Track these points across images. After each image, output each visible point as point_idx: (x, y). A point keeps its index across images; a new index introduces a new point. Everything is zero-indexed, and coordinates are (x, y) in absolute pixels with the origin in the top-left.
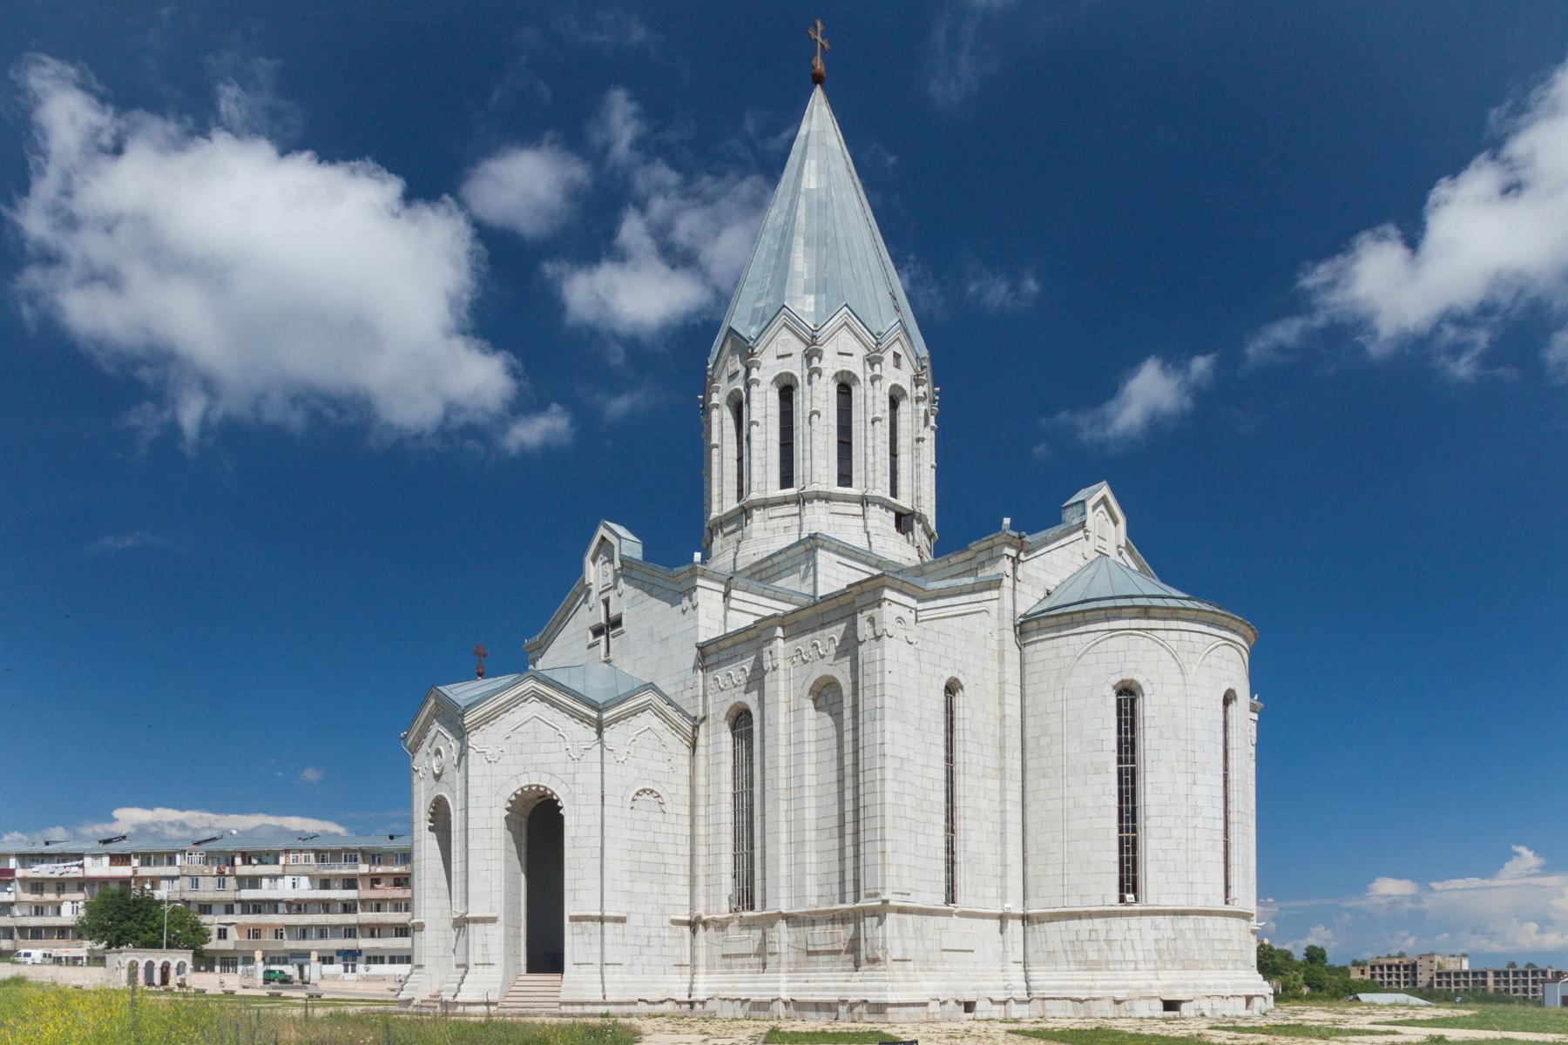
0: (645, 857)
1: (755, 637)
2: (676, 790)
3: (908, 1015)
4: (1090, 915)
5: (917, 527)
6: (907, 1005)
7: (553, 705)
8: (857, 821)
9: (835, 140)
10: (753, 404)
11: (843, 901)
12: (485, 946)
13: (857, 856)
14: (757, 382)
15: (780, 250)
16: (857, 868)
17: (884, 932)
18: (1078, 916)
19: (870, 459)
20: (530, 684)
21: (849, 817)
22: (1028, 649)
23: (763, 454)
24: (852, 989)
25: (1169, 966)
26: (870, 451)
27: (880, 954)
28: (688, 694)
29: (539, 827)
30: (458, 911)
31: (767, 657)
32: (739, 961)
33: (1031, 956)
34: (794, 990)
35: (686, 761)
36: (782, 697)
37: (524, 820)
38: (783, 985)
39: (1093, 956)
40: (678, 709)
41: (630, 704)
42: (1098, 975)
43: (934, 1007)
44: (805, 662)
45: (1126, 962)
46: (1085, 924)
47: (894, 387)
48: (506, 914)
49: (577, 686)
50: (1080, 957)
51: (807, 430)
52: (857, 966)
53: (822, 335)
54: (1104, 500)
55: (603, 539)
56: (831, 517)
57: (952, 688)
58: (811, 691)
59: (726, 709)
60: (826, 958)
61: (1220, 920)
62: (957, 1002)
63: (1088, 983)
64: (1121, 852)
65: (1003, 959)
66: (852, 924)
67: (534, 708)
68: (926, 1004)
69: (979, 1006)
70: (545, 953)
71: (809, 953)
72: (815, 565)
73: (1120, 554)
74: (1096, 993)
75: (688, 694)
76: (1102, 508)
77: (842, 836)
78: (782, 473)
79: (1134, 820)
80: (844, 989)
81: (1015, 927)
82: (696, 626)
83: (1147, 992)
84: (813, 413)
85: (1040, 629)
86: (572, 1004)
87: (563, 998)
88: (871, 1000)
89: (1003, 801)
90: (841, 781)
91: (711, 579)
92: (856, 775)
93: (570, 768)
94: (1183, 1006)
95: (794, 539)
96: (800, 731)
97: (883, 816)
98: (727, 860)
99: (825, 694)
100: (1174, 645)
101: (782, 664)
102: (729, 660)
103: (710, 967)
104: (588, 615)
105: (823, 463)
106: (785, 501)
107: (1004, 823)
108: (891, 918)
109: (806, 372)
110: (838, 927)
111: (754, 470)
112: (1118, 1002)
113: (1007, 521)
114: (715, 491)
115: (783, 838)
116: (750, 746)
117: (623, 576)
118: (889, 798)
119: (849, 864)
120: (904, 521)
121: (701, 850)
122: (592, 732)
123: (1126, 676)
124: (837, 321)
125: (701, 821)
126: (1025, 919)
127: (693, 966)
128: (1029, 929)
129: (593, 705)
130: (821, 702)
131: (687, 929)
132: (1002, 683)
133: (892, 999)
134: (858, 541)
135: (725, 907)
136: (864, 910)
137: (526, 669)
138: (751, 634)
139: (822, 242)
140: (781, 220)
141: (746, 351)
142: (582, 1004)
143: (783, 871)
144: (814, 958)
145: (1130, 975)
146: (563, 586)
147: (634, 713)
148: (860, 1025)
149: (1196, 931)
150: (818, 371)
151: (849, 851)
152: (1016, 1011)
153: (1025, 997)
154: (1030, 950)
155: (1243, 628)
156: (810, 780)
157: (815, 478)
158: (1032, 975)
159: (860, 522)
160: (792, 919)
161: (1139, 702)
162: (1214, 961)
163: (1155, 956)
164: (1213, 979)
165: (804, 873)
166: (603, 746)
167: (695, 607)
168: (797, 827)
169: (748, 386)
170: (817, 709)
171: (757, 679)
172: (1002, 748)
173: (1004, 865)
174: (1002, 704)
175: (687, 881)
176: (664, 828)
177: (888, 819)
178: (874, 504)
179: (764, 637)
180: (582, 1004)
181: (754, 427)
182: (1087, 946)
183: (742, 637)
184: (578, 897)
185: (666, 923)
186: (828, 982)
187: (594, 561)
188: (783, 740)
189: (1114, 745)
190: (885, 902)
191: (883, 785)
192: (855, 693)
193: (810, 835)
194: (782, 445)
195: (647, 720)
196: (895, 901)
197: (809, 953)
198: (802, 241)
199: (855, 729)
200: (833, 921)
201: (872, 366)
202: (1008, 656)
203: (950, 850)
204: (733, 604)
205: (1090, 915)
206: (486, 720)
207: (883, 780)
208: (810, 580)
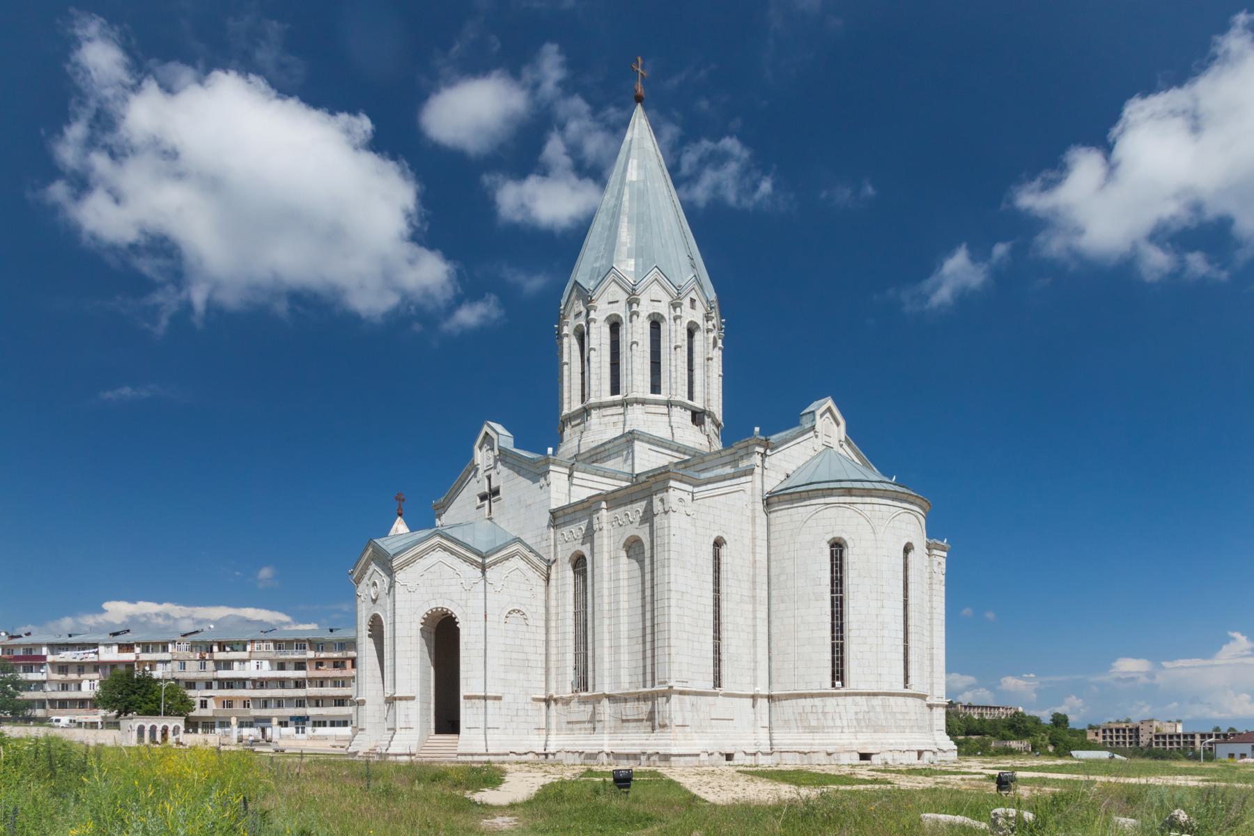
0: (514, 655)
1: (587, 508)
4: (812, 696)
5: (708, 420)
7: (452, 553)
12: (407, 716)
13: (653, 657)
16: (653, 664)
18: (804, 696)
19: (673, 375)
20: (437, 539)
21: (648, 630)
22: (772, 515)
26: (673, 369)
27: (667, 722)
28: (544, 544)
29: (443, 635)
30: (389, 692)
31: (595, 521)
32: (578, 726)
33: (774, 724)
35: (542, 590)
36: (605, 548)
37: (433, 631)
39: (814, 723)
40: (537, 555)
41: (504, 552)
42: (817, 736)
43: (704, 757)
46: (809, 701)
47: (691, 323)
49: (468, 540)
50: (806, 724)
52: (653, 729)
53: (639, 289)
54: (829, 410)
55: (487, 433)
57: (718, 543)
58: (625, 545)
60: (634, 724)
61: (901, 699)
65: (754, 725)
66: (650, 701)
68: (698, 755)
69: (736, 757)
70: (447, 721)
71: (623, 721)
72: (633, 452)
74: (815, 748)
75: (544, 544)
76: (828, 415)
77: (644, 643)
78: (612, 384)
81: (763, 703)
84: (633, 343)
88: (661, 752)
89: (755, 618)
90: (643, 606)
91: (560, 465)
92: (653, 603)
93: (464, 596)
94: (873, 757)
95: (619, 433)
96: (617, 572)
98: (570, 657)
99: (633, 547)
100: (868, 513)
101: (605, 526)
102: (571, 522)
103: (559, 730)
104: (477, 486)
105: (641, 377)
106: (614, 404)
107: (755, 633)
108: (674, 698)
111: (592, 382)
112: (829, 754)
114: (566, 395)
115: (607, 643)
118: (673, 619)
119: (649, 662)
120: (698, 417)
121: (553, 651)
123: (836, 535)
124: (650, 278)
125: (553, 631)
127: (548, 729)
129: (479, 554)
130: (631, 553)
131: (543, 705)
132: (754, 539)
133: (674, 751)
134: (664, 433)
135: (569, 689)
137: (433, 525)
138: (586, 505)
139: (642, 222)
140: (612, 202)
141: (587, 298)
142: (472, 755)
143: (606, 666)
145: (838, 736)
147: (507, 558)
149: (883, 706)
151: (649, 653)
154: (773, 719)
155: (918, 501)
156: (624, 605)
157: (635, 389)
159: (666, 418)
160: (612, 698)
162: (896, 727)
163: (855, 723)
164: (895, 739)
168: (616, 636)
169: (588, 323)
171: (589, 536)
172: (754, 582)
173: (755, 662)
174: (754, 553)
175: (543, 671)
176: (527, 636)
180: (472, 755)
183: (580, 507)
184: (469, 683)
185: (529, 700)
188: (606, 577)
190: (671, 687)
192: (652, 548)
193: (624, 642)
195: (516, 562)
197: (623, 721)
199: (652, 572)
200: (638, 700)
201: (675, 309)
202: (758, 521)
203: (717, 651)
204: (575, 481)
205: (812, 696)
206: (407, 563)
208: (630, 462)
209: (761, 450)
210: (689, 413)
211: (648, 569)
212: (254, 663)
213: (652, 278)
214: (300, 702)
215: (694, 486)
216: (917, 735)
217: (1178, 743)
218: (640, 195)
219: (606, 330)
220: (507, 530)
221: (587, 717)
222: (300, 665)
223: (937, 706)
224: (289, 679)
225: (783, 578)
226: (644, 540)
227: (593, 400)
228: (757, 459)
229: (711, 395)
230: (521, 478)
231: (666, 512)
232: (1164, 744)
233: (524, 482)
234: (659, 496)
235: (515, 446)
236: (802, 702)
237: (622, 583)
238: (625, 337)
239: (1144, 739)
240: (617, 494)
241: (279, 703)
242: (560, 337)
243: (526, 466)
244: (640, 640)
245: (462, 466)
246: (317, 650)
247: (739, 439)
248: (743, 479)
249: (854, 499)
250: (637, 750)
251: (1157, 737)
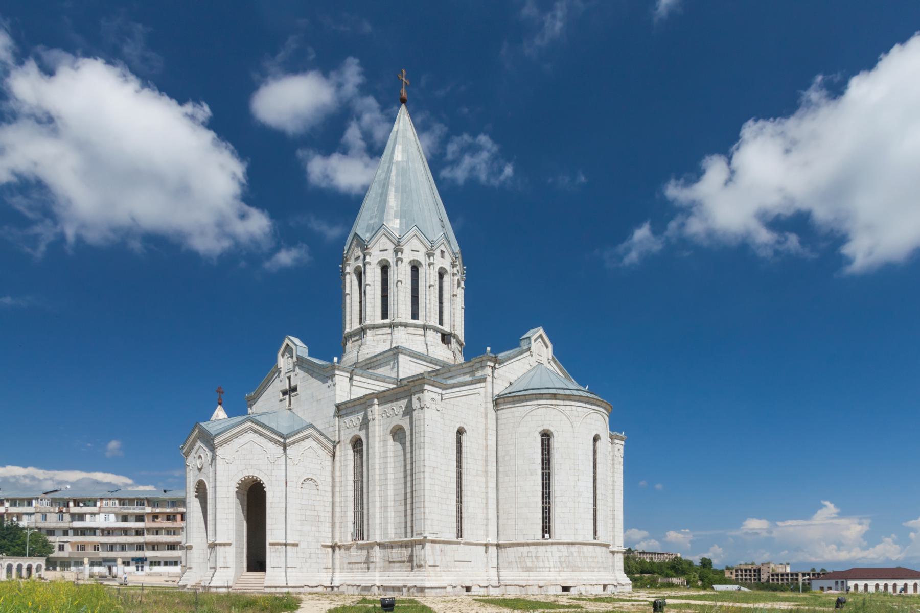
0: (308, 513)
1: (364, 403)
3: (436, 593)
4: (528, 544)
5: (453, 341)
7: (261, 435)
9: (412, 134)
10: (367, 274)
12: (225, 558)
13: (412, 515)
14: (369, 263)
15: (382, 193)
16: (412, 520)
18: (522, 545)
19: (428, 306)
21: (409, 495)
22: (500, 412)
27: (423, 563)
28: (331, 429)
29: (253, 497)
30: (211, 540)
31: (369, 413)
32: (356, 566)
35: (330, 464)
36: (377, 434)
37: (246, 493)
39: (529, 564)
40: (326, 437)
42: (531, 574)
43: (449, 589)
46: (526, 549)
47: (441, 268)
48: (236, 541)
49: (273, 425)
50: (524, 565)
52: (412, 568)
57: (460, 432)
58: (391, 432)
66: (409, 548)
67: (251, 436)
69: (473, 589)
70: (257, 563)
72: (398, 362)
74: (530, 583)
75: (331, 429)
77: (406, 504)
78: (383, 311)
81: (493, 549)
83: (554, 582)
84: (398, 281)
85: (505, 403)
86: (270, 587)
87: (266, 585)
88: (418, 585)
89: (487, 487)
90: (405, 477)
91: (343, 371)
92: (412, 475)
95: (388, 348)
96: (386, 451)
98: (350, 514)
99: (398, 433)
101: (377, 417)
103: (342, 569)
104: (278, 385)
105: (404, 307)
106: (384, 326)
107: (487, 498)
108: (428, 545)
109: (395, 260)
111: (368, 309)
112: (540, 587)
113: (489, 349)
115: (378, 504)
118: (427, 487)
120: (446, 338)
121: (337, 509)
122: (281, 449)
124: (411, 234)
125: (337, 494)
126: (498, 546)
129: (281, 436)
130: (396, 437)
131: (330, 550)
132: (486, 429)
133: (428, 584)
134: (421, 349)
135: (349, 538)
137: (246, 413)
138: (362, 401)
139: (405, 191)
140: (383, 176)
142: (275, 587)
143: (378, 521)
147: (303, 439)
151: (409, 512)
154: (500, 561)
156: (391, 476)
157: (399, 315)
159: (423, 338)
160: (381, 545)
161: (552, 440)
165: (387, 522)
168: (384, 499)
169: (365, 265)
171: (365, 424)
172: (486, 461)
173: (487, 519)
174: (486, 440)
175: (330, 525)
180: (275, 587)
181: (368, 287)
182: (527, 560)
184: (274, 532)
185: (319, 546)
188: (377, 455)
190: (425, 538)
192: (412, 434)
193: (391, 503)
195: (310, 443)
196: (430, 537)
199: (412, 452)
200: (401, 546)
201: (429, 257)
202: (489, 416)
203: (459, 511)
204: (354, 383)
205: (528, 544)
208: (395, 369)
209: (492, 364)
210: (440, 335)
211: (408, 449)
212: (102, 516)
213: (413, 234)
214: (140, 547)
215: (443, 389)
217: (787, 580)
218: (404, 172)
219: (378, 271)
220: (303, 418)
221: (363, 559)
222: (140, 518)
223: (618, 552)
224: (130, 529)
225: (507, 458)
227: (368, 322)
228: (488, 371)
229: (456, 322)
230: (314, 380)
231: (422, 408)
232: (778, 580)
233: (316, 383)
234: (417, 396)
235: (309, 355)
236: (521, 549)
237: (389, 460)
238: (392, 277)
239: (764, 577)
240: (386, 394)
241: (123, 547)
242: (344, 274)
243: (317, 371)
244: (403, 502)
245: (269, 369)
248: (478, 385)
250: (400, 584)
251: (773, 575)
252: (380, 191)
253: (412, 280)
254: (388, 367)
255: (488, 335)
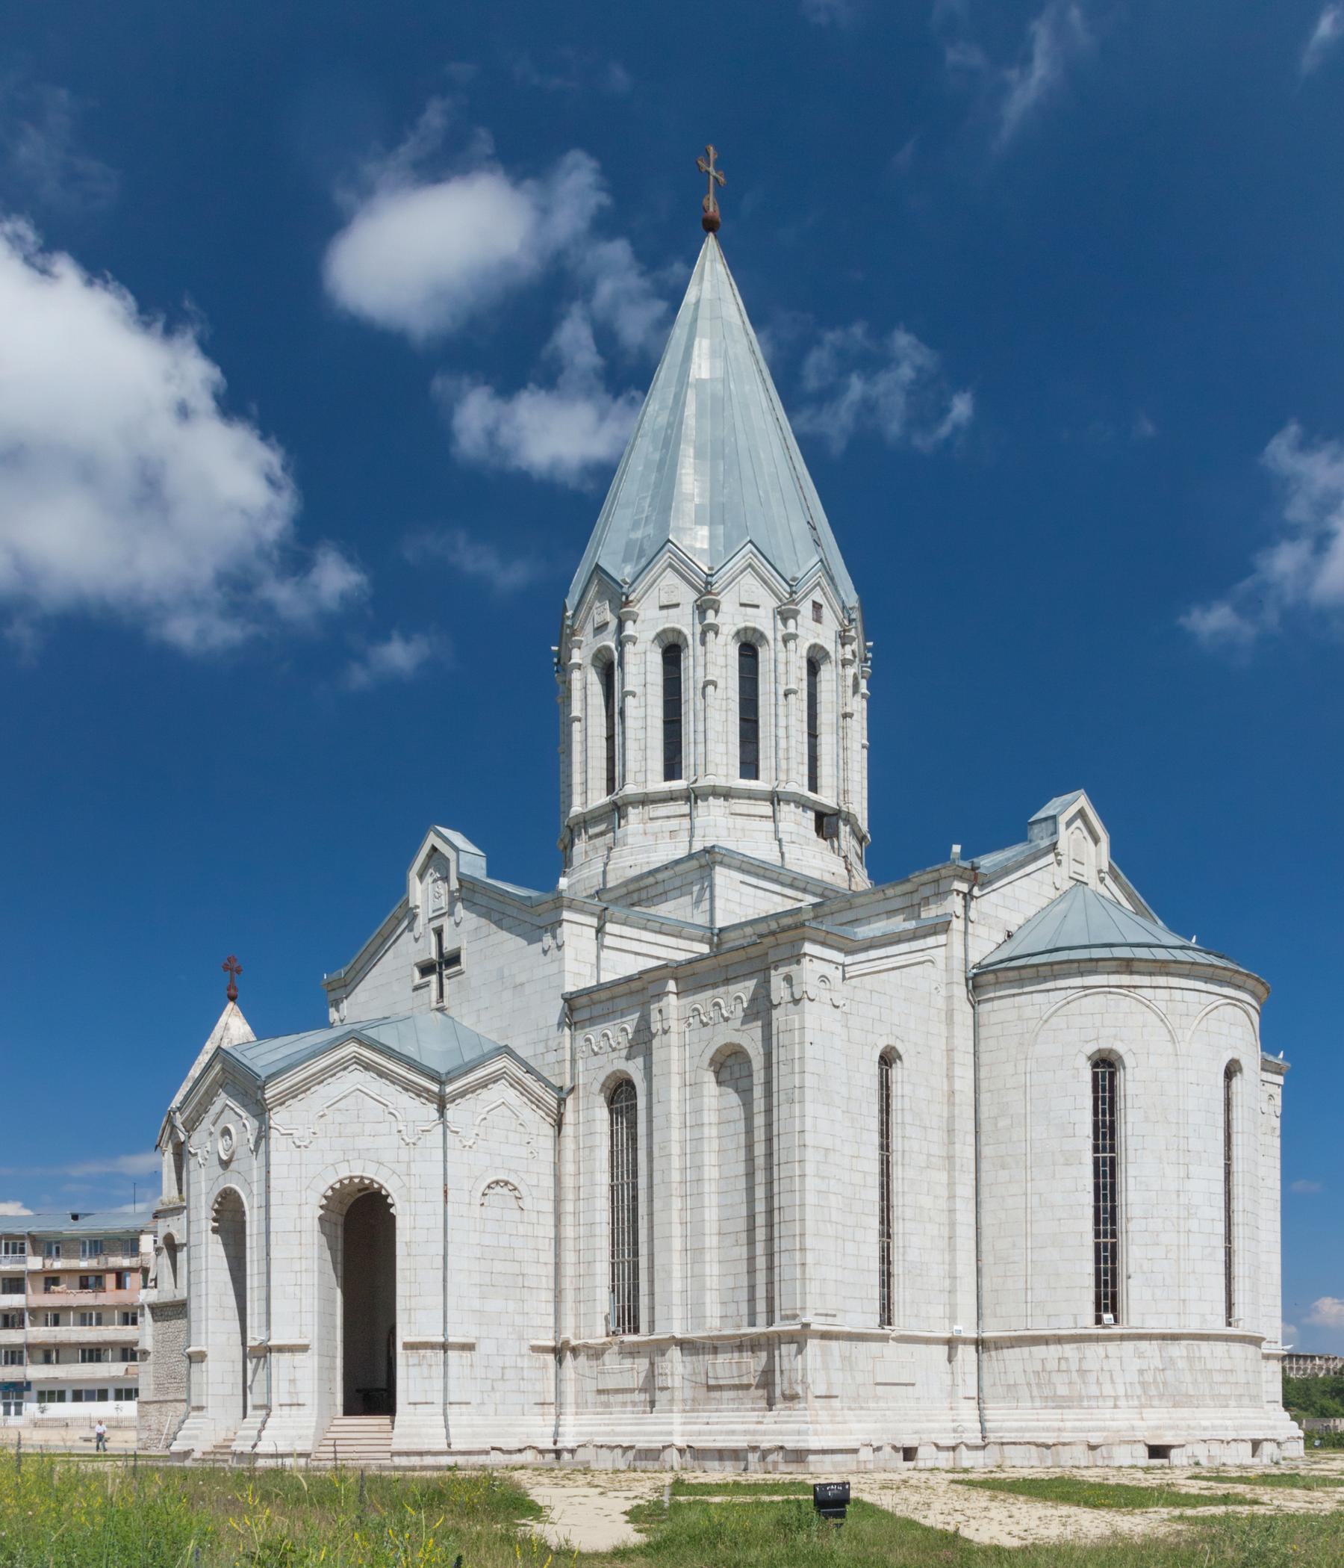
0: (498, 1267)
1: (639, 992)
2: (537, 1181)
3: (834, 1464)
4: (1059, 1340)
6: (833, 1452)
7: (381, 1074)
8: (770, 1225)
10: (628, 668)
11: (752, 1324)
12: (293, 1381)
13: (770, 1268)
14: (633, 640)
15: (661, 463)
16: (770, 1283)
17: (804, 1361)
20: (351, 1049)
21: (760, 1220)
22: (984, 1008)
23: (641, 735)
24: (765, 1433)
25: (1156, 1402)
27: (799, 1389)
28: (551, 1057)
29: (362, 1227)
31: (655, 1016)
34: (691, 1434)
35: (548, 1143)
36: (675, 1067)
37: (341, 1220)
38: (677, 1428)
39: (1062, 1390)
40: (540, 1078)
42: (1069, 1414)
43: (866, 1454)
44: (705, 1025)
45: (1104, 1397)
46: (1054, 1350)
47: (814, 648)
48: (320, 1339)
49: (409, 1050)
50: (1047, 1392)
51: (700, 705)
52: (770, 1404)
54: (1081, 814)
55: (434, 849)
56: (731, 819)
57: (888, 1059)
58: (712, 1062)
59: (602, 1078)
60: (732, 1394)
61: (1220, 1347)
62: (895, 1448)
63: (1056, 1424)
64: (1097, 1261)
65: (952, 1394)
66: (764, 1351)
68: (855, 1451)
70: (370, 1390)
71: (710, 1388)
72: (712, 886)
73: (1102, 880)
74: (1066, 1437)
75: (551, 1057)
76: (1079, 823)
77: (751, 1242)
79: (1114, 1222)
80: (754, 1433)
81: (967, 1354)
82: (561, 972)
83: (1128, 1436)
85: (998, 984)
86: (407, 1454)
87: (395, 1447)
89: (952, 1197)
90: (750, 1175)
92: (769, 1168)
93: (404, 1155)
94: (1173, 1452)
95: (681, 852)
96: (698, 1111)
97: (803, 1220)
99: (729, 1066)
105: (721, 748)
106: (671, 797)
107: (952, 1225)
108: (813, 1345)
109: (698, 629)
110: (747, 1356)
111: (631, 755)
112: (1092, 1448)
114: (577, 778)
115: (677, 1244)
116: (633, 1125)
117: (463, 900)
118: (811, 1199)
119: (761, 1278)
121: (569, 1257)
122: (432, 1110)
123: (1104, 1045)
124: (739, 562)
125: (568, 1220)
126: (980, 1344)
127: (559, 1404)
128: (985, 1356)
130: (725, 1075)
131: (550, 1358)
132: (950, 1051)
133: (814, 1443)
134: (764, 851)
136: (779, 1334)
138: (635, 985)
139: (719, 455)
140: (663, 419)
141: (619, 598)
142: (421, 1454)
143: (677, 1285)
144: (716, 1394)
145: (1108, 1413)
146: (381, 910)
147: (484, 1084)
148: (777, 1476)
149: (1189, 1359)
150: (714, 629)
151: (761, 1262)
152: (967, 1459)
153: (980, 1442)
156: (711, 1172)
157: (711, 769)
158: (989, 1414)
159: (769, 825)
160: (686, 1346)
163: (1139, 1391)
164: (1211, 1419)
165: (702, 1289)
166: (445, 1127)
167: (559, 947)
168: (694, 1231)
169: (621, 644)
170: (719, 1083)
171: (642, 1043)
172: (951, 1131)
173: (953, 1278)
174: (950, 1077)
176: (522, 1230)
177: (810, 1225)
178: (788, 802)
179: (653, 990)
180: (421, 1454)
181: (629, 700)
182: (1057, 1378)
184: (414, 1318)
185: (525, 1350)
186: (735, 1424)
187: (421, 876)
188: (676, 1121)
189: (1089, 1129)
190: (806, 1325)
191: (803, 1183)
193: (711, 1241)
194: (666, 723)
195: (501, 1092)
197: (710, 1388)
198: (691, 451)
199: (769, 1111)
200: (740, 1348)
201: (785, 621)
202: (958, 1017)
203: (886, 1259)
204: (608, 941)
205: (1059, 1340)
206: (294, 1093)
207: (803, 1176)
208: (705, 905)
209: (964, 887)
210: (811, 815)
211: (759, 1105)
213: (743, 564)
215: (848, 952)
216: (1249, 1412)
219: (656, 658)
220: (480, 1029)
226: (752, 1053)
227: (631, 789)
228: (956, 904)
229: (847, 783)
230: (505, 935)
231: (796, 1002)
233: (511, 942)
234: (783, 970)
235: (489, 875)
236: (1040, 1351)
237: (706, 1131)
240: (699, 967)
242: (563, 667)
246: (48, 1255)
247: (922, 865)
248: (931, 941)
249: (1137, 980)
250: (740, 1442)
252: (657, 456)
253: (742, 679)
254: (686, 900)
255: (932, 817)
